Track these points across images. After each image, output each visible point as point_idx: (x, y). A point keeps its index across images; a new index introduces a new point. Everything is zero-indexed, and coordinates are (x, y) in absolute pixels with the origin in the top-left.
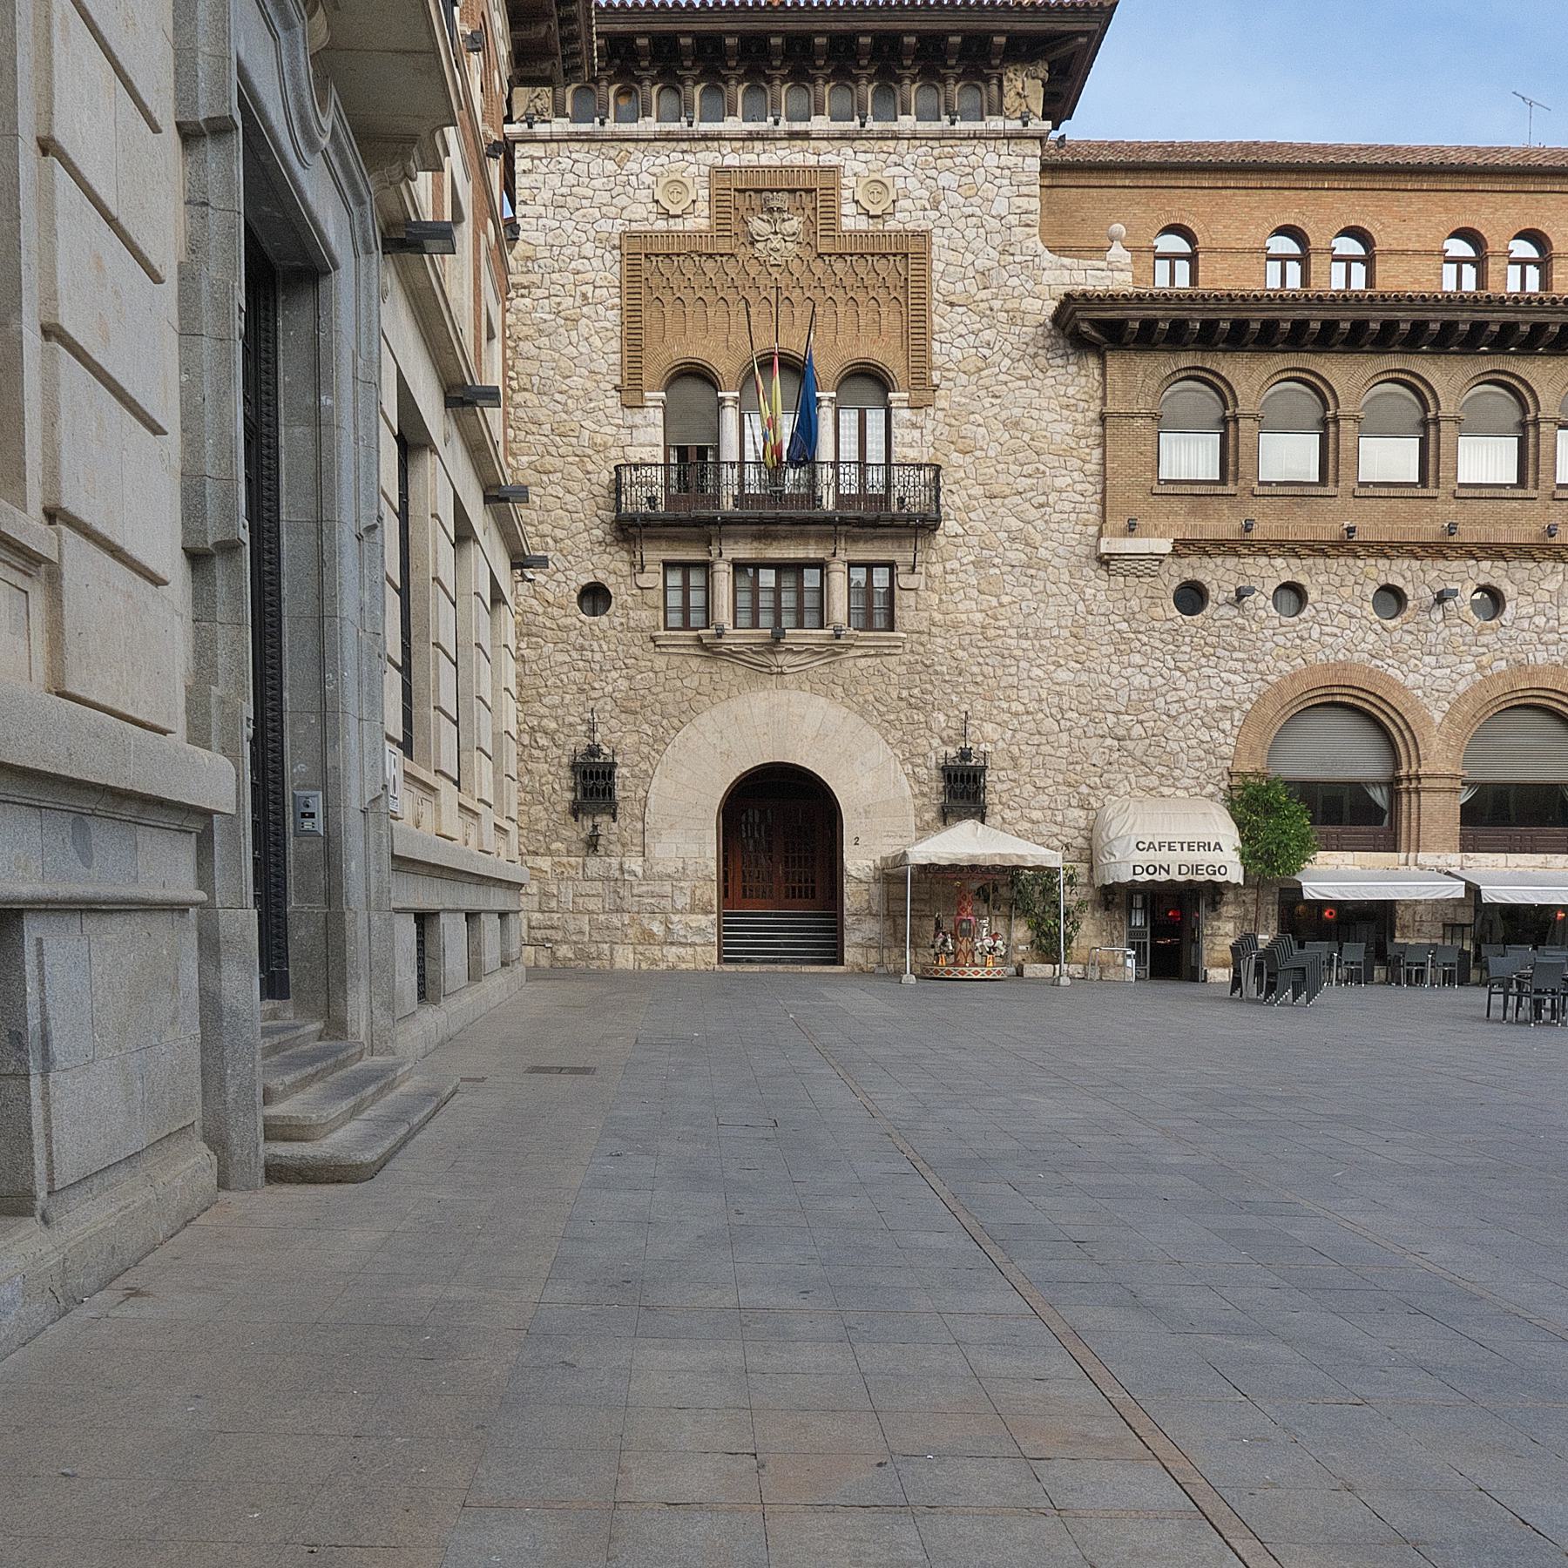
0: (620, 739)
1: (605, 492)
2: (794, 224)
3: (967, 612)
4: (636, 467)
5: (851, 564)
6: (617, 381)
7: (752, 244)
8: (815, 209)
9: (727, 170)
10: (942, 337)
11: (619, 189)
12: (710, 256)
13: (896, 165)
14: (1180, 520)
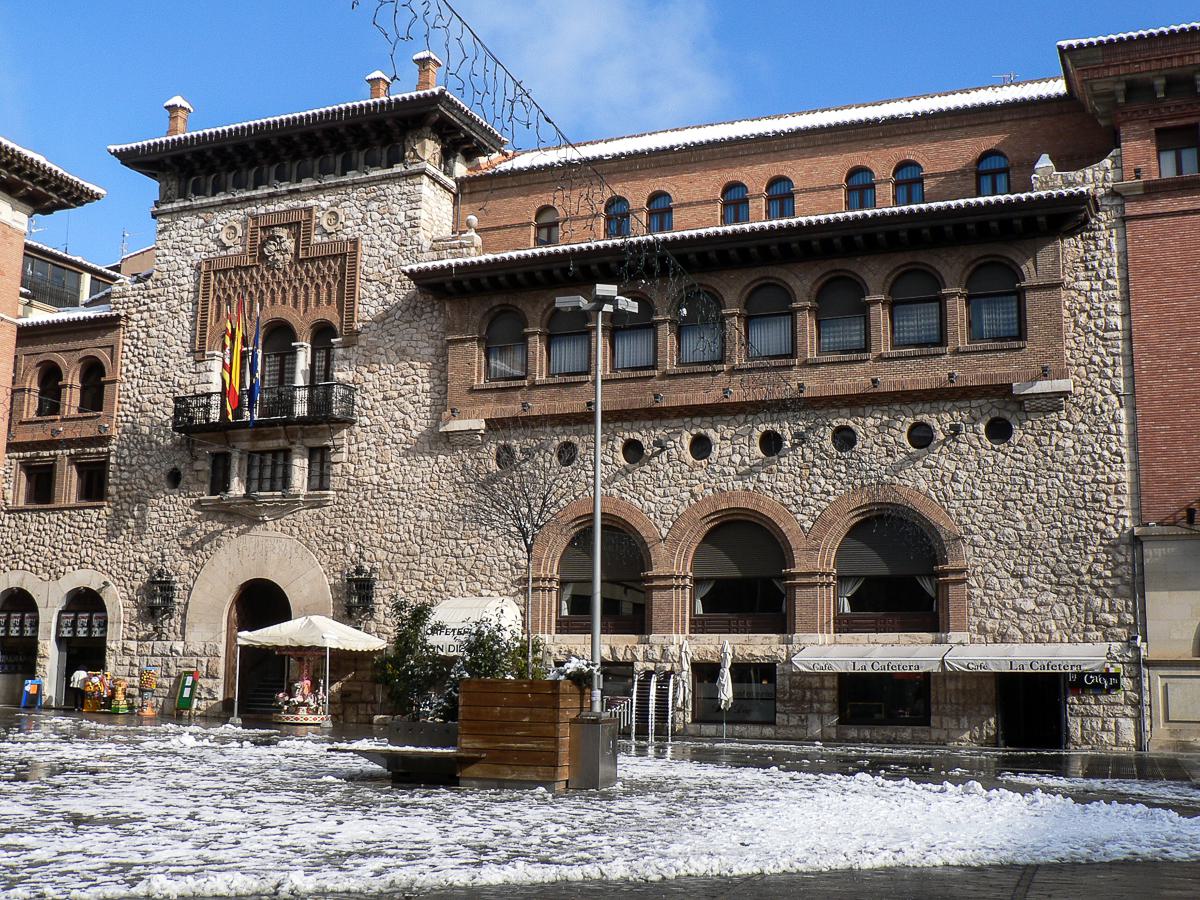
0: (179, 565)
14: (491, 406)
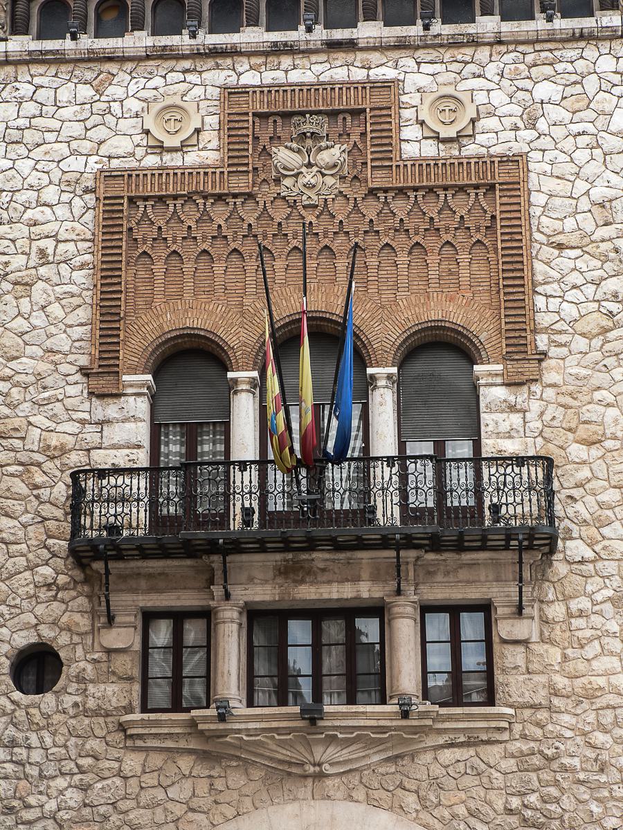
1: (59, 513)
2: (333, 154)
3: (607, 674)
4: (102, 474)
5: (426, 609)
6: (84, 361)
7: (277, 181)
8: (363, 134)
9: (243, 91)
10: (548, 289)
11: (96, 119)
12: (220, 198)
13: (476, 76)
